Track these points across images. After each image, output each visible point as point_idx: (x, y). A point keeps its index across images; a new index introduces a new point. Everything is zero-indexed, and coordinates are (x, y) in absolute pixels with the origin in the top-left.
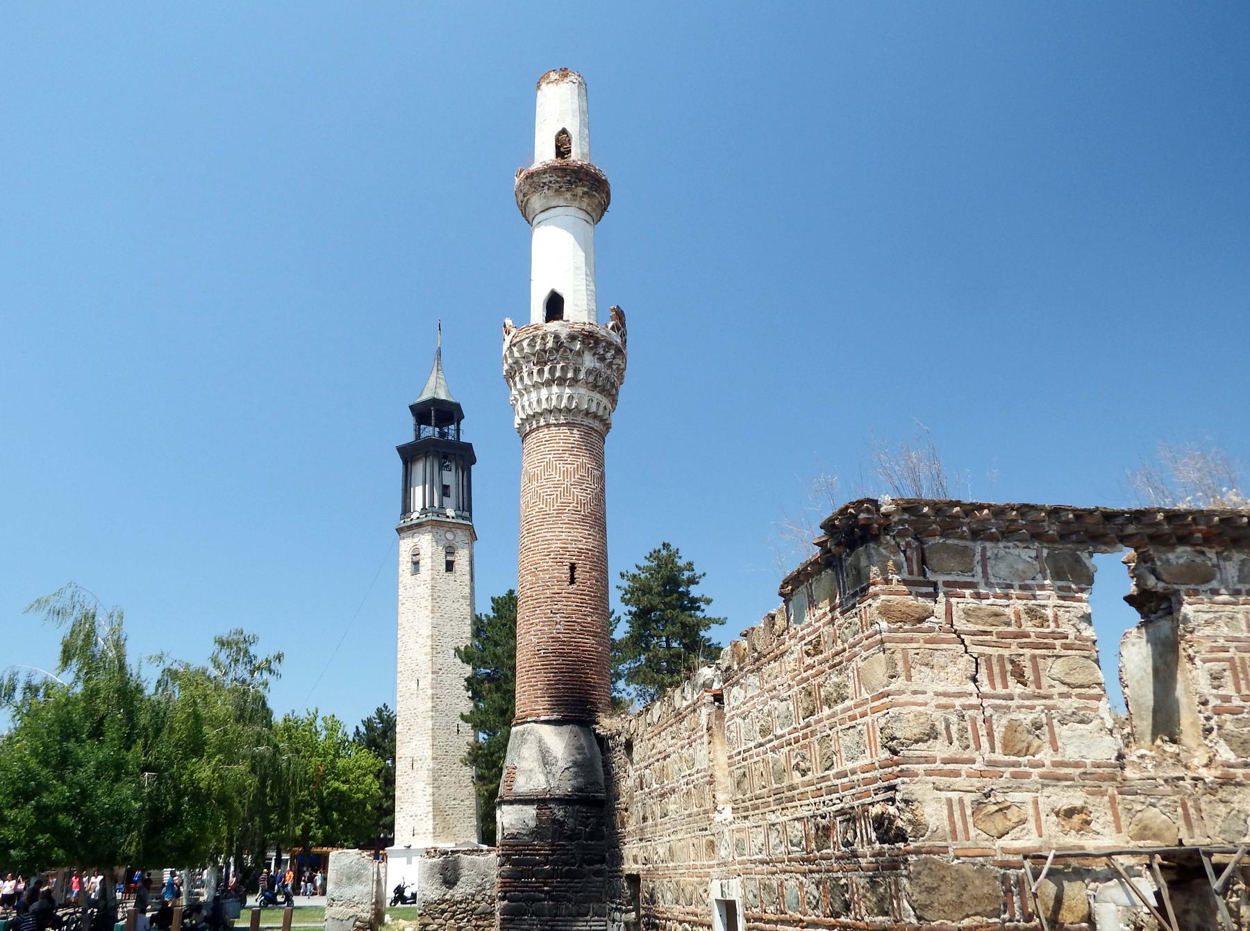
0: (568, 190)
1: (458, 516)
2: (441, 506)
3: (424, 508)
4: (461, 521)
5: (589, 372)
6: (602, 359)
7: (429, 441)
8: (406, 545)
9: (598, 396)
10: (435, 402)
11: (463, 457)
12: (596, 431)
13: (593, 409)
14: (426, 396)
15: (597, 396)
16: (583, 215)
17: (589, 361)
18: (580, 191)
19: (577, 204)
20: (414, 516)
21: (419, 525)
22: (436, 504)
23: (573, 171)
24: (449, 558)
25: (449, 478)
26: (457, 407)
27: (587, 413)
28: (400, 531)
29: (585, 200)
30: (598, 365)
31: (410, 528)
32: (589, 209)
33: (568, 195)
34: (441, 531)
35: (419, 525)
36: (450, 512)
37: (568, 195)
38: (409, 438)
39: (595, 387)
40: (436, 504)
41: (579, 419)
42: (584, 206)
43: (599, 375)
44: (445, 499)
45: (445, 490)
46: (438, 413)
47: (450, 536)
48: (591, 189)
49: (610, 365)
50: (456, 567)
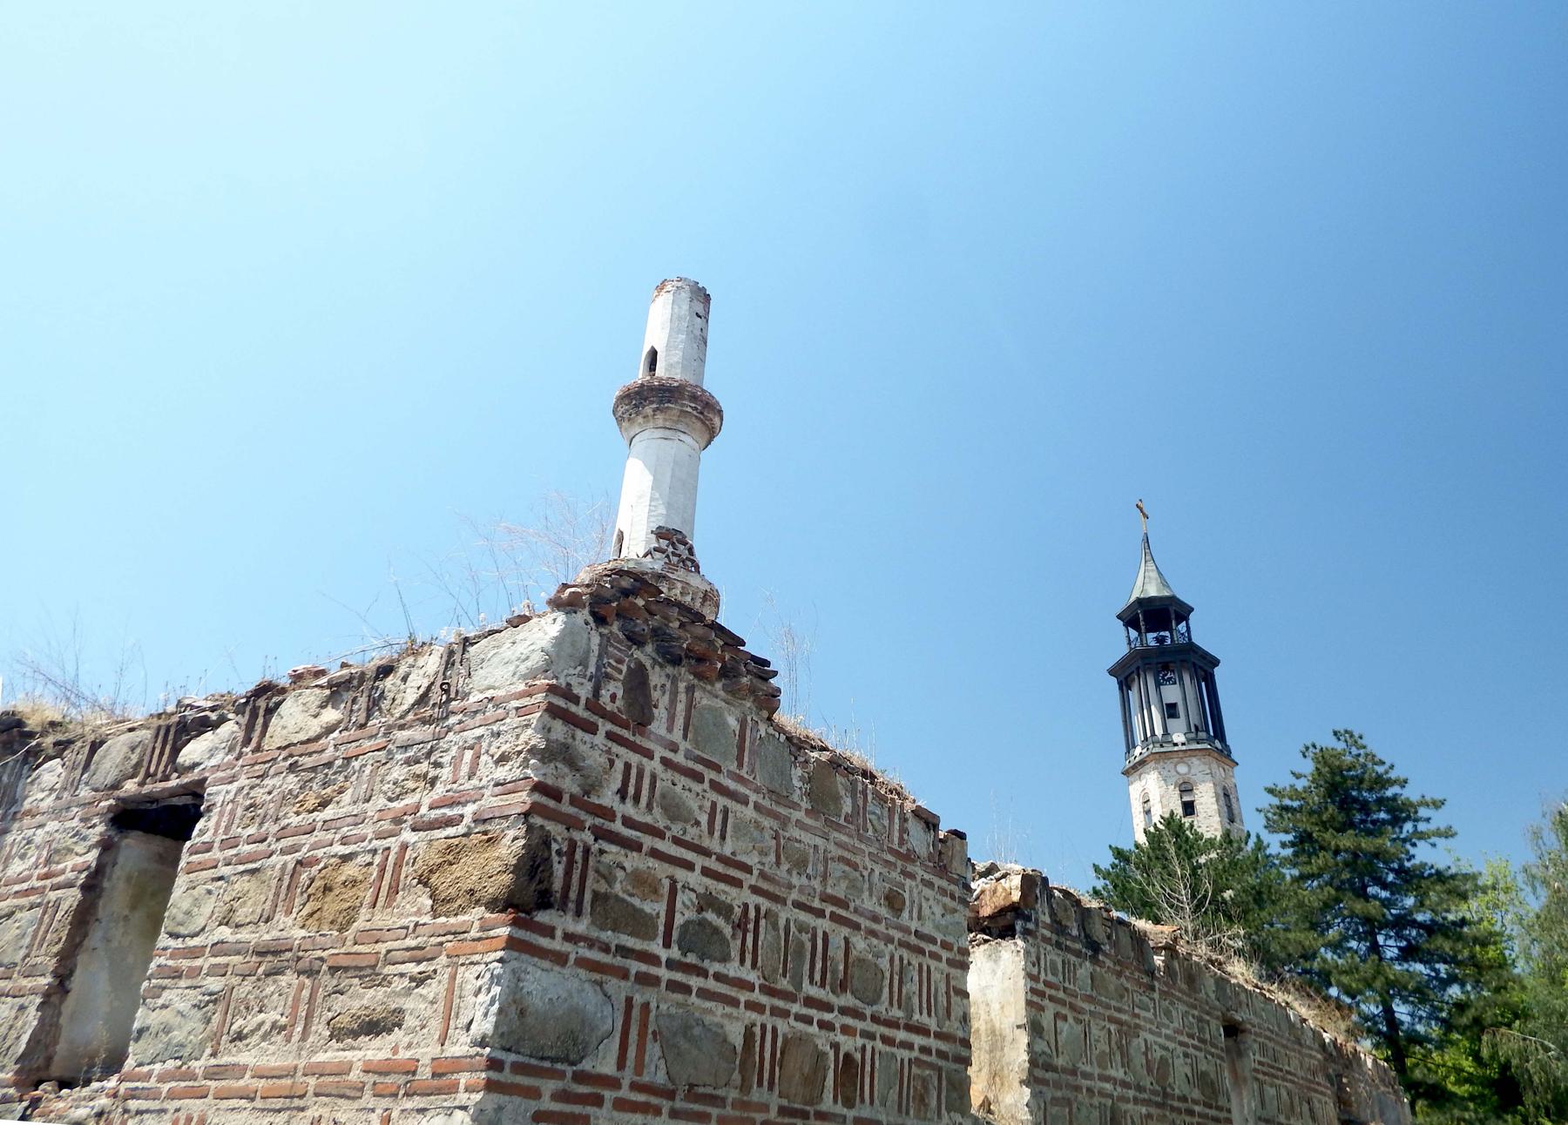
0: (637, 414)
1: (1189, 741)
2: (1166, 733)
3: (1146, 739)
4: (1195, 746)
8: (1135, 790)
10: (1139, 601)
14: (1133, 599)
16: (660, 433)
18: (648, 410)
19: (651, 425)
20: (1138, 750)
21: (1142, 763)
22: (1159, 731)
23: (637, 393)
24: (1186, 799)
25: (1172, 693)
26: (1173, 600)
28: (1126, 773)
29: (659, 416)
31: (1135, 768)
32: (668, 424)
33: (640, 419)
34: (1169, 765)
35: (1142, 763)
36: (1179, 738)
37: (640, 419)
38: (1122, 650)
42: (660, 423)
44: (1170, 722)
45: (1171, 711)
46: (1155, 614)
47: (1182, 769)
48: (661, 402)
50: (1198, 807)
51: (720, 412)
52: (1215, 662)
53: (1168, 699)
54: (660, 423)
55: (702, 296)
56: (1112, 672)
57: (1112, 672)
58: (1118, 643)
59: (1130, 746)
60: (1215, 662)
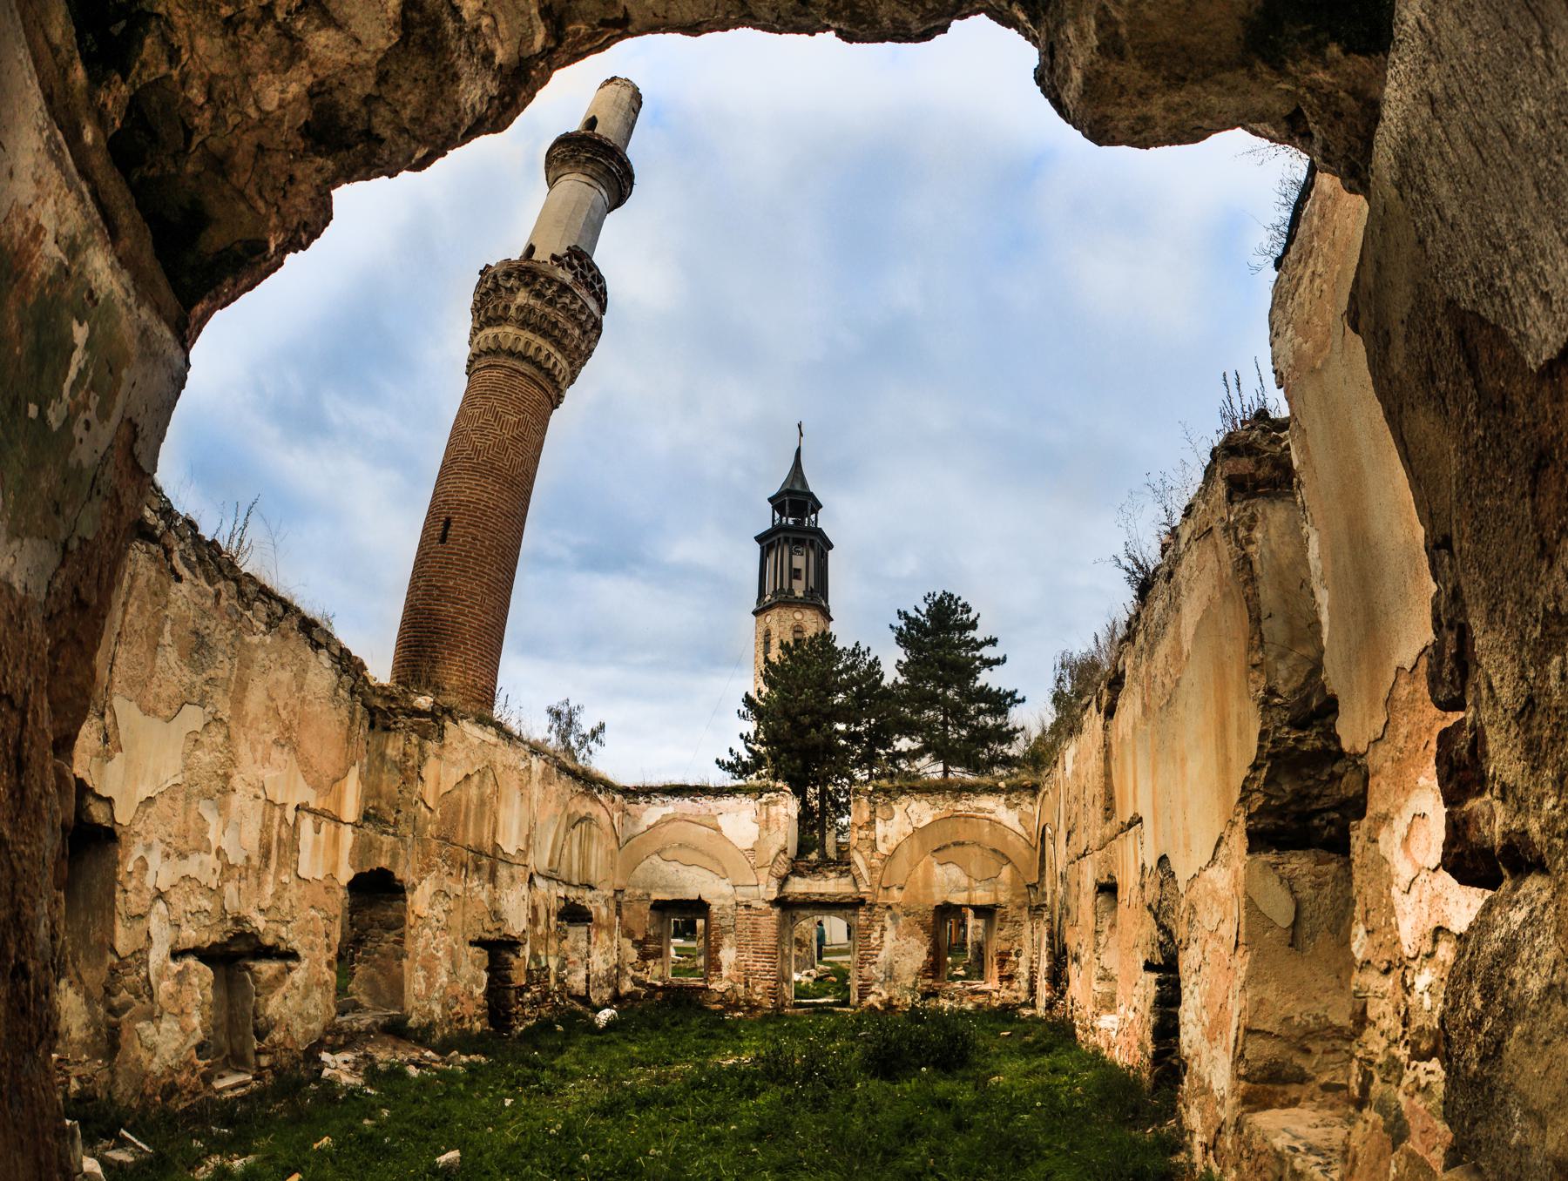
5: (520, 309)
6: (539, 295)
7: (786, 528)
9: (530, 336)
11: (820, 545)
12: (523, 374)
13: (521, 347)
15: (527, 335)
16: (583, 178)
17: (522, 297)
18: (583, 156)
22: (786, 586)
24: (798, 636)
27: (511, 353)
30: (532, 302)
39: (524, 324)
40: (786, 586)
41: (501, 361)
42: (589, 171)
43: (532, 310)
47: (798, 616)
49: (551, 302)
51: (632, 184)
52: (830, 546)
53: (795, 565)
54: (589, 171)
55: (637, 98)
56: (759, 539)
57: (759, 539)
58: (764, 518)
59: (762, 593)
60: (830, 546)
